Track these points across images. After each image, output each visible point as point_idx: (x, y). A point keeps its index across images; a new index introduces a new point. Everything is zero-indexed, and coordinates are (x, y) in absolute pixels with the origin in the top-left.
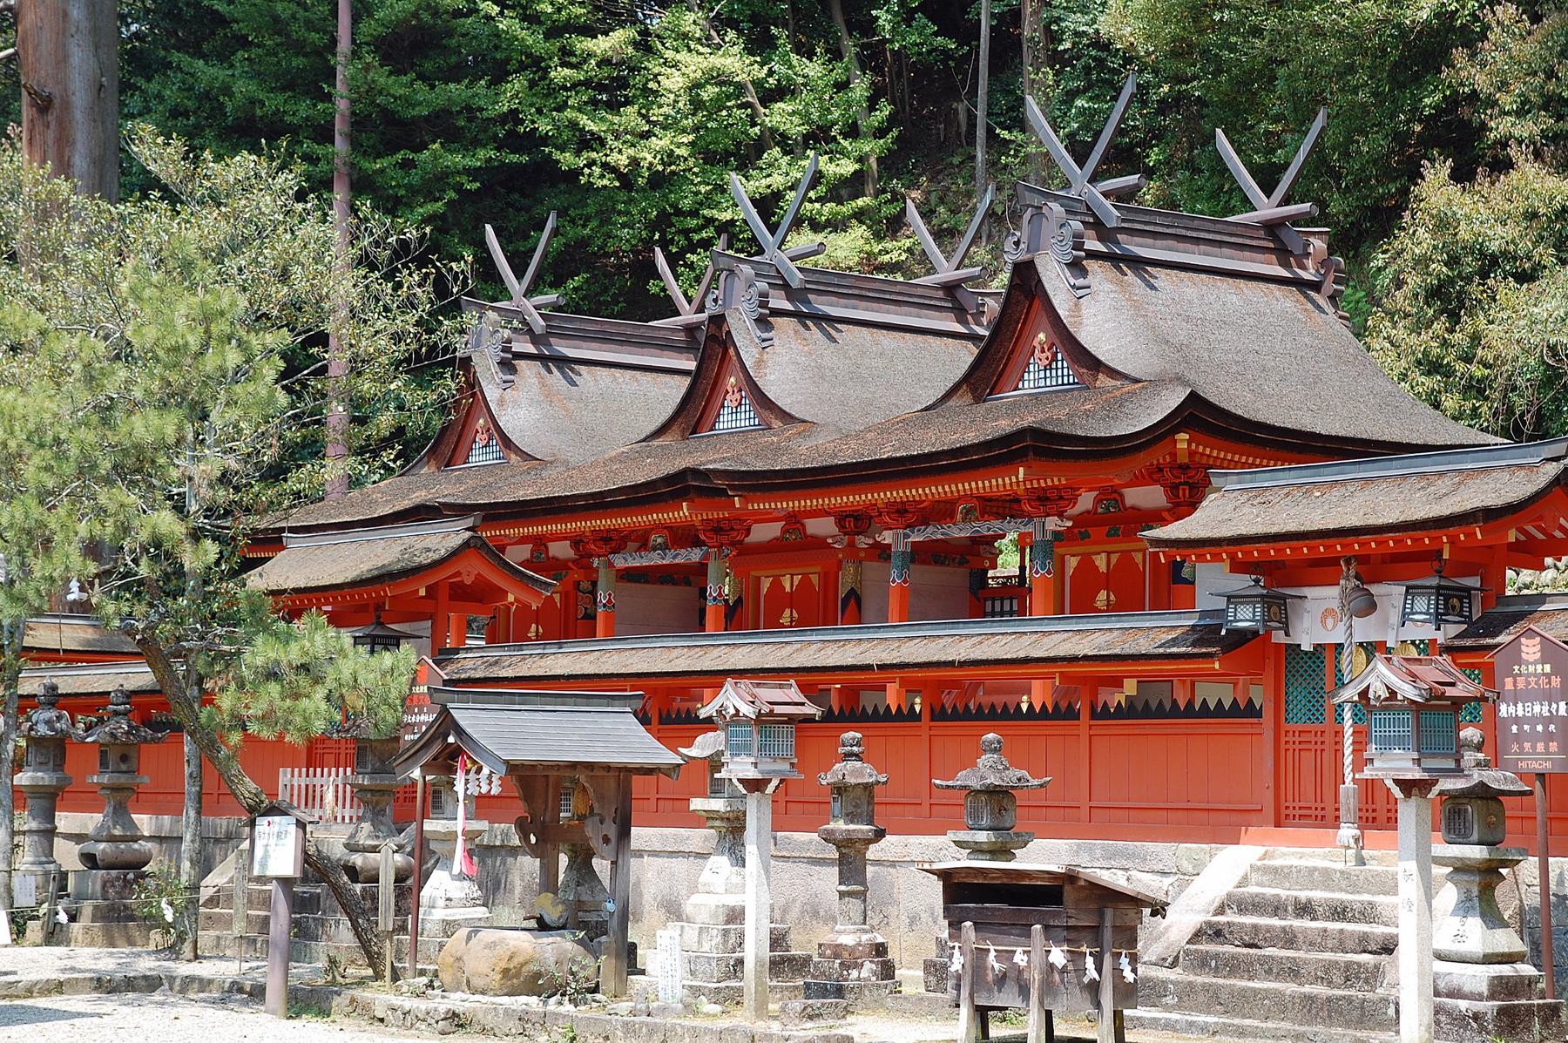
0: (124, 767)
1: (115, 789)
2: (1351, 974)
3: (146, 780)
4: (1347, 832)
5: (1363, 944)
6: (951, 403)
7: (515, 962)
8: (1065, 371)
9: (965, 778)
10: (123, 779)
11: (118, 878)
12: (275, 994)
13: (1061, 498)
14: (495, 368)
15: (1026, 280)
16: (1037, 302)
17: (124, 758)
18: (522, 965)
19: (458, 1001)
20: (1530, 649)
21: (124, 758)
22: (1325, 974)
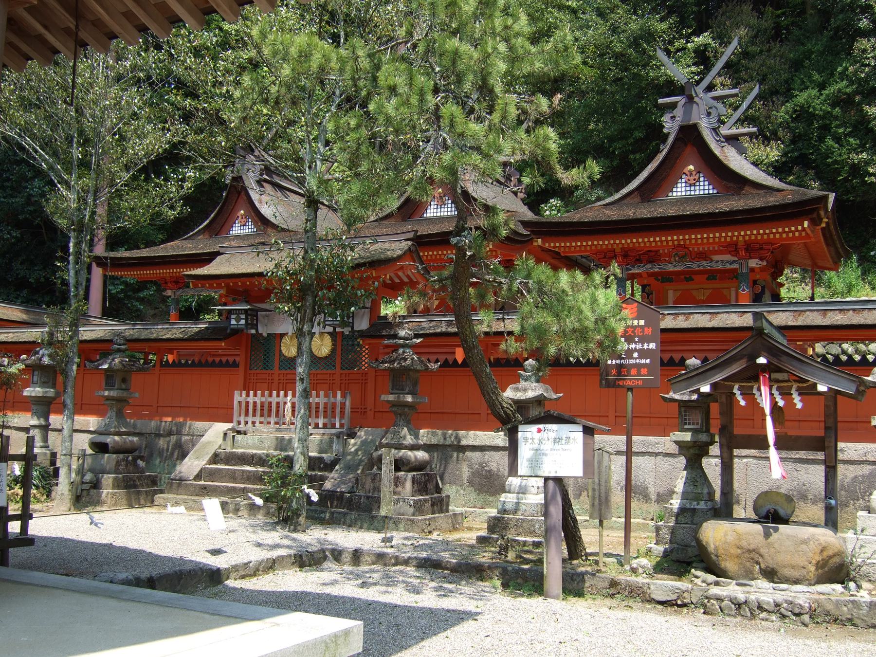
0: (124, 386)
1: (119, 400)
3: (137, 395)
6: (625, 201)
7: (825, 554)
8: (704, 188)
10: (125, 394)
11: (123, 460)
13: (761, 249)
14: (254, 185)
17: (124, 380)
18: (831, 557)
21: (124, 380)
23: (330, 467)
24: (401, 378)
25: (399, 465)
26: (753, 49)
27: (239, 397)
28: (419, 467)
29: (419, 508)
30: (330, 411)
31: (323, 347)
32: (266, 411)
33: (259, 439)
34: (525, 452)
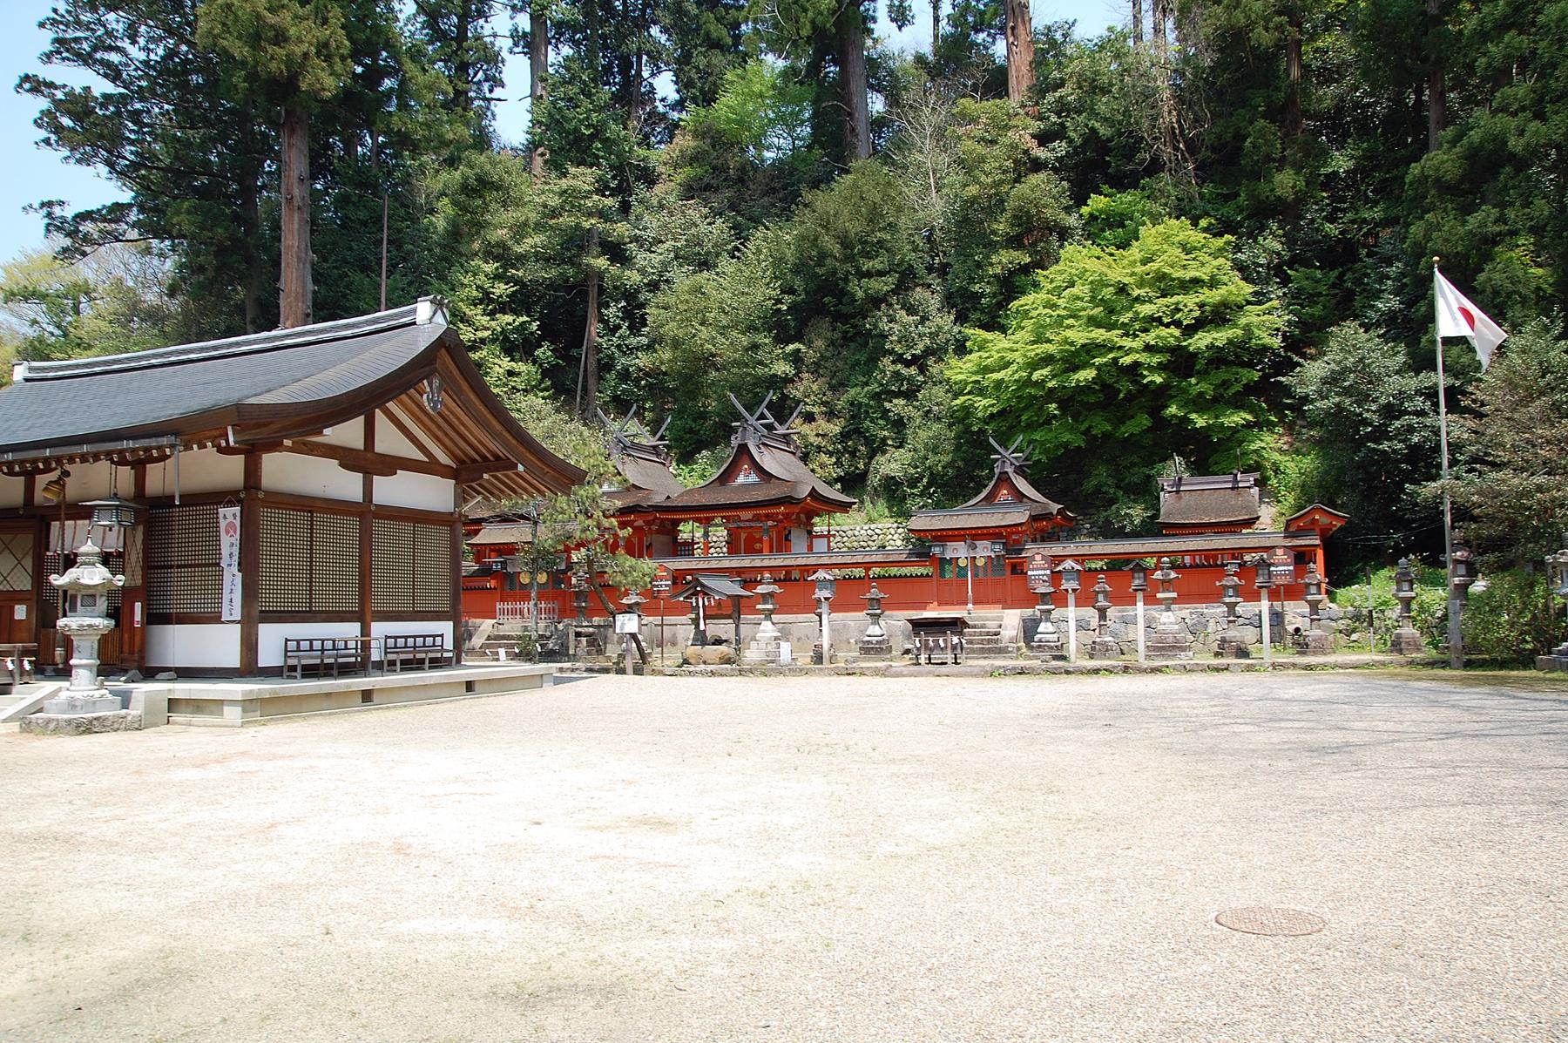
2: (989, 641)
4: (970, 606)
5: (988, 634)
8: (753, 478)
9: (868, 596)
12: (630, 669)
15: (743, 449)
16: (745, 457)
19: (710, 668)
20: (1038, 558)
22: (982, 642)
23: (548, 638)
24: (579, 595)
25: (578, 634)
26: (828, 354)
27: (499, 606)
28: (588, 635)
29: (589, 653)
30: (548, 611)
31: (542, 578)
32: (514, 612)
33: (512, 626)
34: (618, 624)
